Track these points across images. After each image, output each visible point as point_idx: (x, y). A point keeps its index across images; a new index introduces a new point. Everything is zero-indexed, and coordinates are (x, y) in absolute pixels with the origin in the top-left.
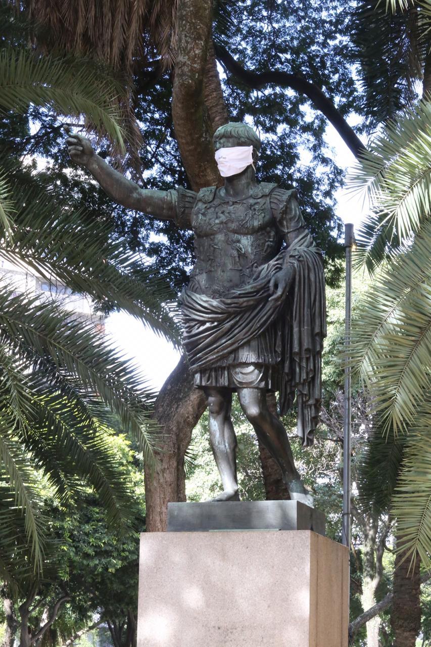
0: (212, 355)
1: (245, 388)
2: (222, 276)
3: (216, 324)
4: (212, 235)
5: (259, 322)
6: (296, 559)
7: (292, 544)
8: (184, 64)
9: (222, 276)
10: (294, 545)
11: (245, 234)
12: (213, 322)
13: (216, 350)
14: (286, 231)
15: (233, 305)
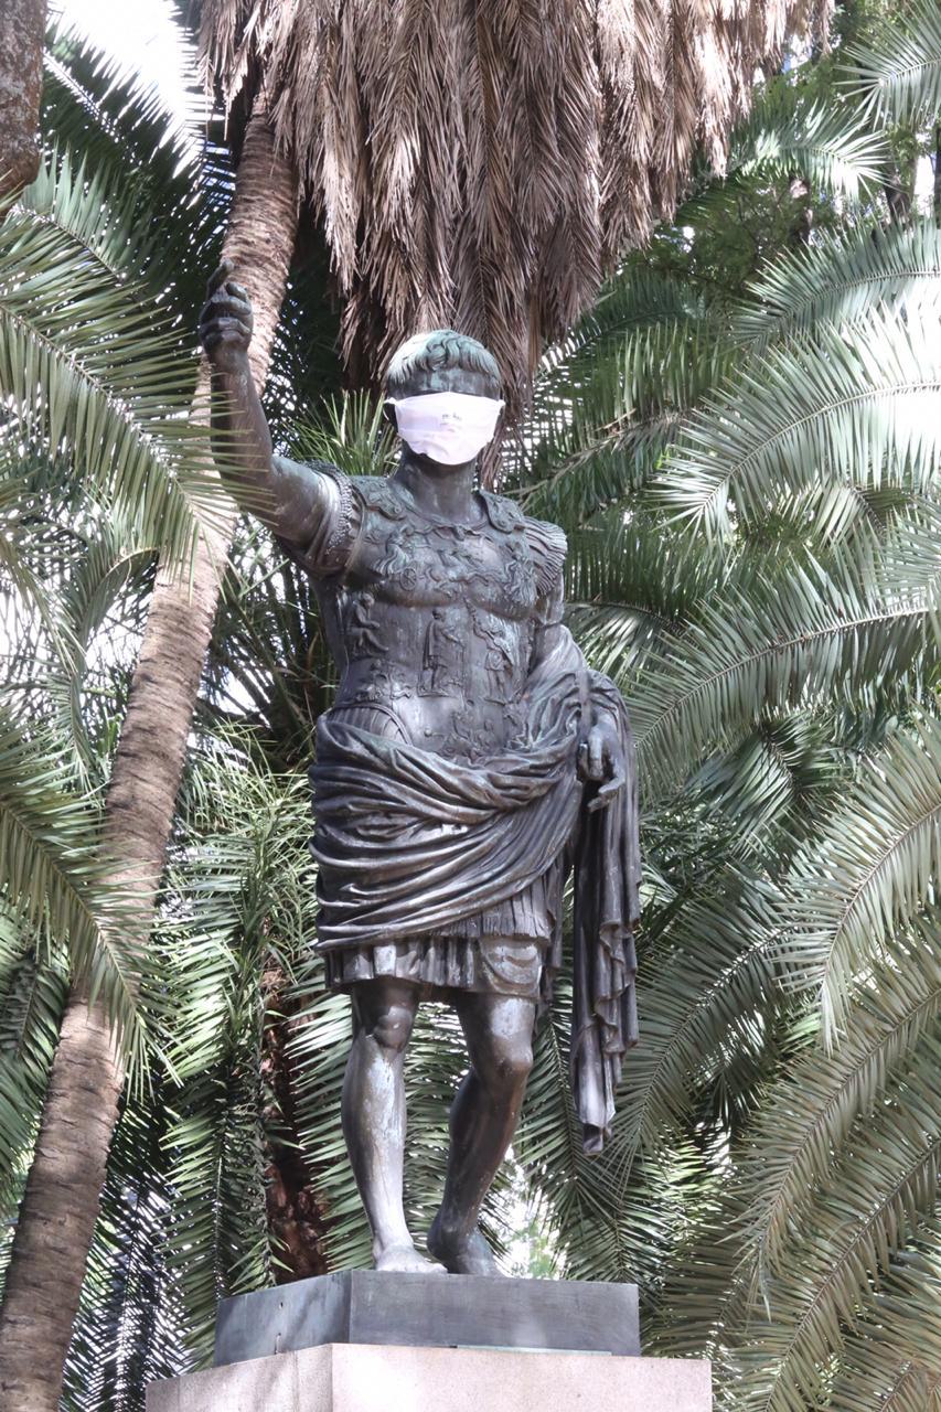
1: (513, 996)
2: (470, 714)
3: (464, 829)
7: (673, 1392)
8: (17, 100)
11: (509, 618)
12: (458, 826)
14: (545, 623)
15: (513, 791)
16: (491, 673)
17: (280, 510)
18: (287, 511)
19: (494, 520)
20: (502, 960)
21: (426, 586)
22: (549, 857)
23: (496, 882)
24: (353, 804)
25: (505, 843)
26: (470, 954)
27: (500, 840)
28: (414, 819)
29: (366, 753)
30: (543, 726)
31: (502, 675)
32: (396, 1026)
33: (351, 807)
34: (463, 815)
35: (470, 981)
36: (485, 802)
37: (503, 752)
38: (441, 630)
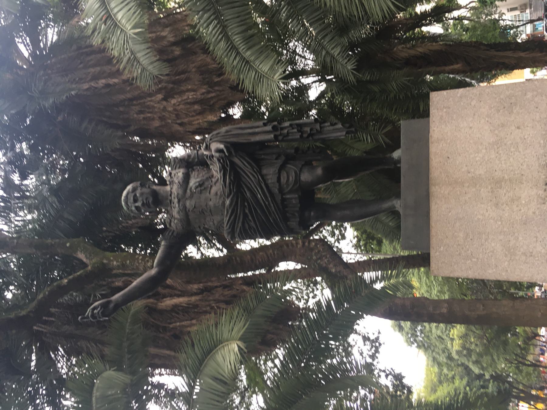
0: (270, 207)
1: (300, 179)
3: (246, 204)
4: (186, 210)
5: (247, 167)
6: (462, 104)
7: (445, 110)
10: (446, 108)
13: (267, 203)
15: (232, 188)
26: (288, 196)
38: (192, 211)
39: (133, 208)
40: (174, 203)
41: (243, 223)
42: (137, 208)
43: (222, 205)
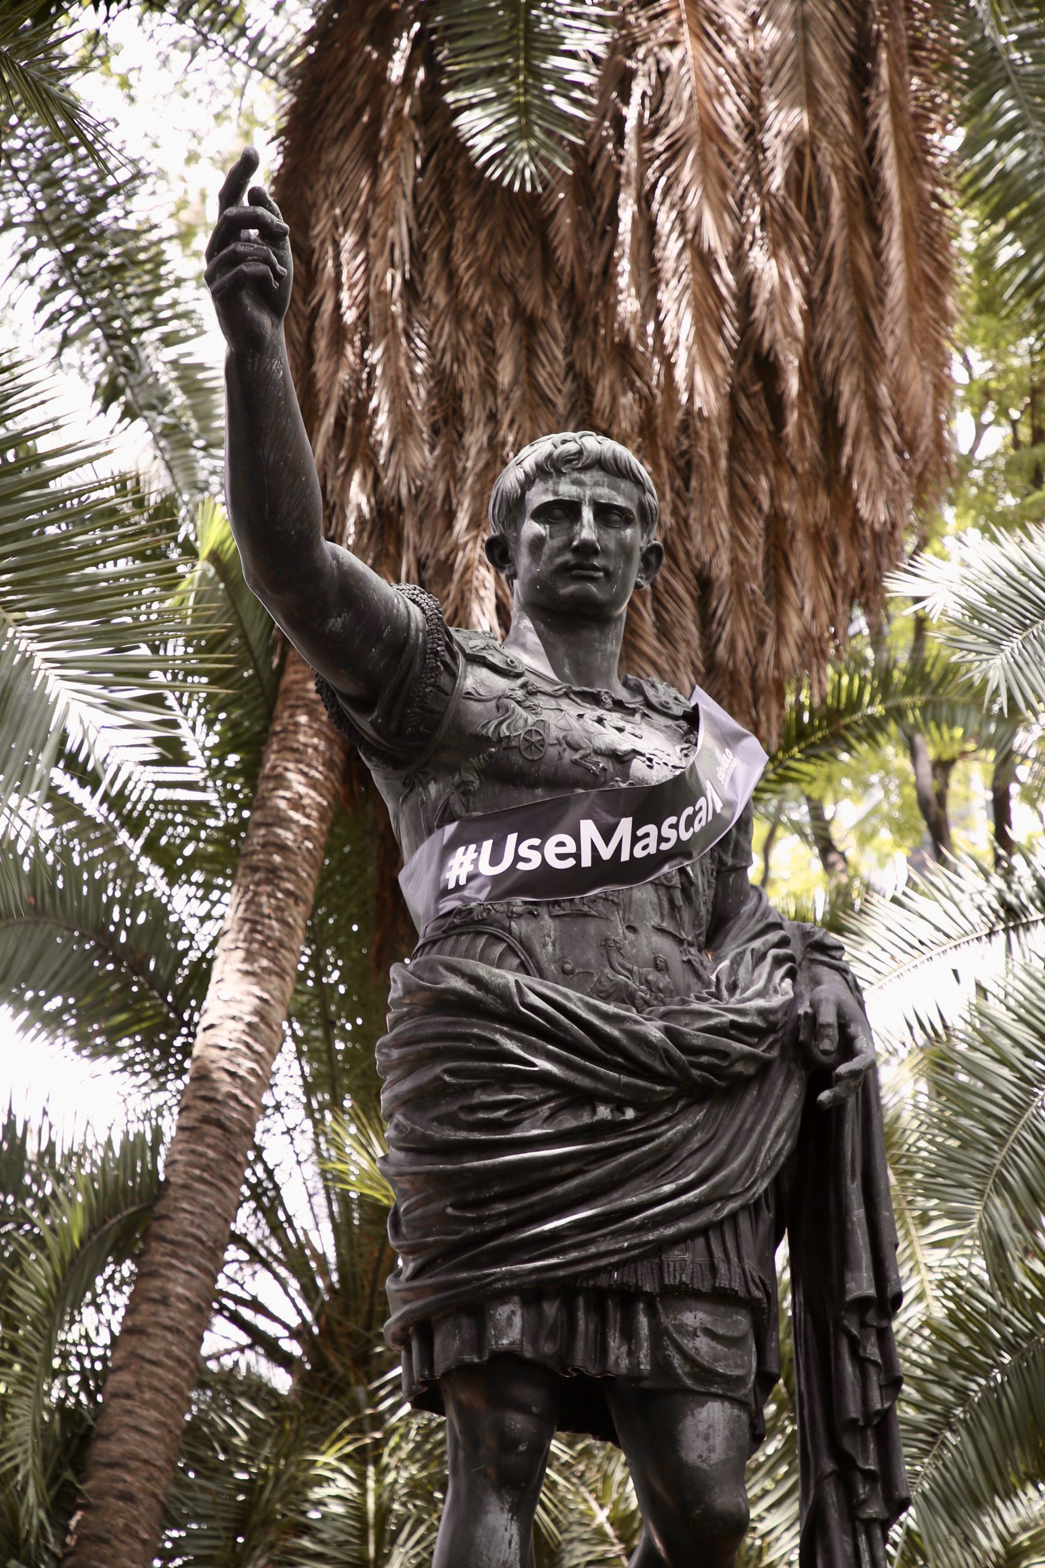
1: (715, 1396)
2: (631, 943)
9: (631, 943)
15: (704, 1059)
16: (662, 892)
17: (336, 623)
18: (344, 626)
19: (654, 700)
20: (695, 1335)
21: (560, 757)
22: (762, 1175)
23: (684, 1198)
24: (448, 1071)
25: (695, 1144)
27: (687, 1136)
28: (552, 1092)
29: (470, 990)
30: (741, 984)
31: (678, 894)
32: (522, 1448)
33: (447, 1078)
34: (628, 1086)
35: (645, 1367)
36: (661, 1069)
37: (684, 1002)
39: (567, 489)
40: (600, 721)
41: (544, 1079)
42: (569, 510)
43: (616, 985)
